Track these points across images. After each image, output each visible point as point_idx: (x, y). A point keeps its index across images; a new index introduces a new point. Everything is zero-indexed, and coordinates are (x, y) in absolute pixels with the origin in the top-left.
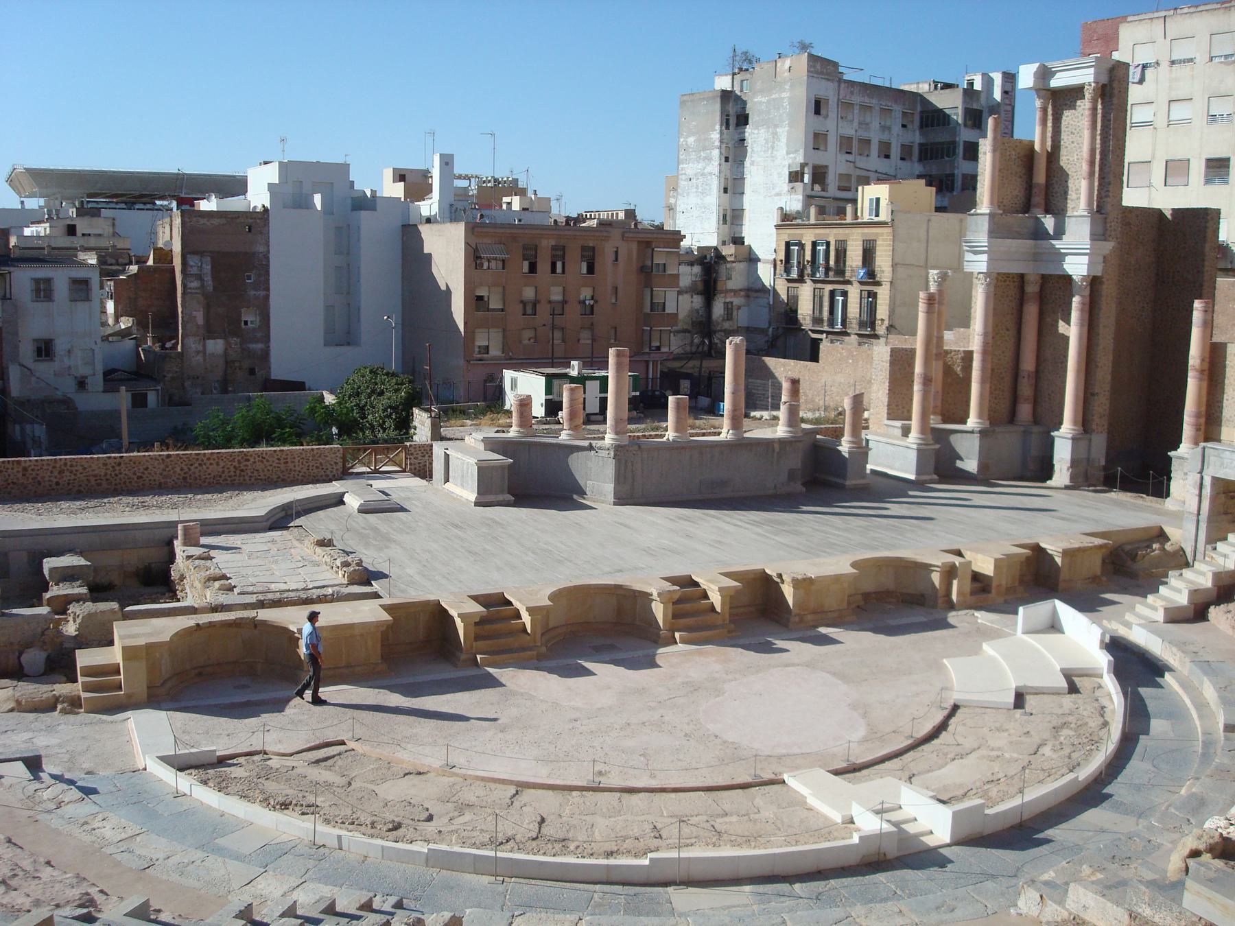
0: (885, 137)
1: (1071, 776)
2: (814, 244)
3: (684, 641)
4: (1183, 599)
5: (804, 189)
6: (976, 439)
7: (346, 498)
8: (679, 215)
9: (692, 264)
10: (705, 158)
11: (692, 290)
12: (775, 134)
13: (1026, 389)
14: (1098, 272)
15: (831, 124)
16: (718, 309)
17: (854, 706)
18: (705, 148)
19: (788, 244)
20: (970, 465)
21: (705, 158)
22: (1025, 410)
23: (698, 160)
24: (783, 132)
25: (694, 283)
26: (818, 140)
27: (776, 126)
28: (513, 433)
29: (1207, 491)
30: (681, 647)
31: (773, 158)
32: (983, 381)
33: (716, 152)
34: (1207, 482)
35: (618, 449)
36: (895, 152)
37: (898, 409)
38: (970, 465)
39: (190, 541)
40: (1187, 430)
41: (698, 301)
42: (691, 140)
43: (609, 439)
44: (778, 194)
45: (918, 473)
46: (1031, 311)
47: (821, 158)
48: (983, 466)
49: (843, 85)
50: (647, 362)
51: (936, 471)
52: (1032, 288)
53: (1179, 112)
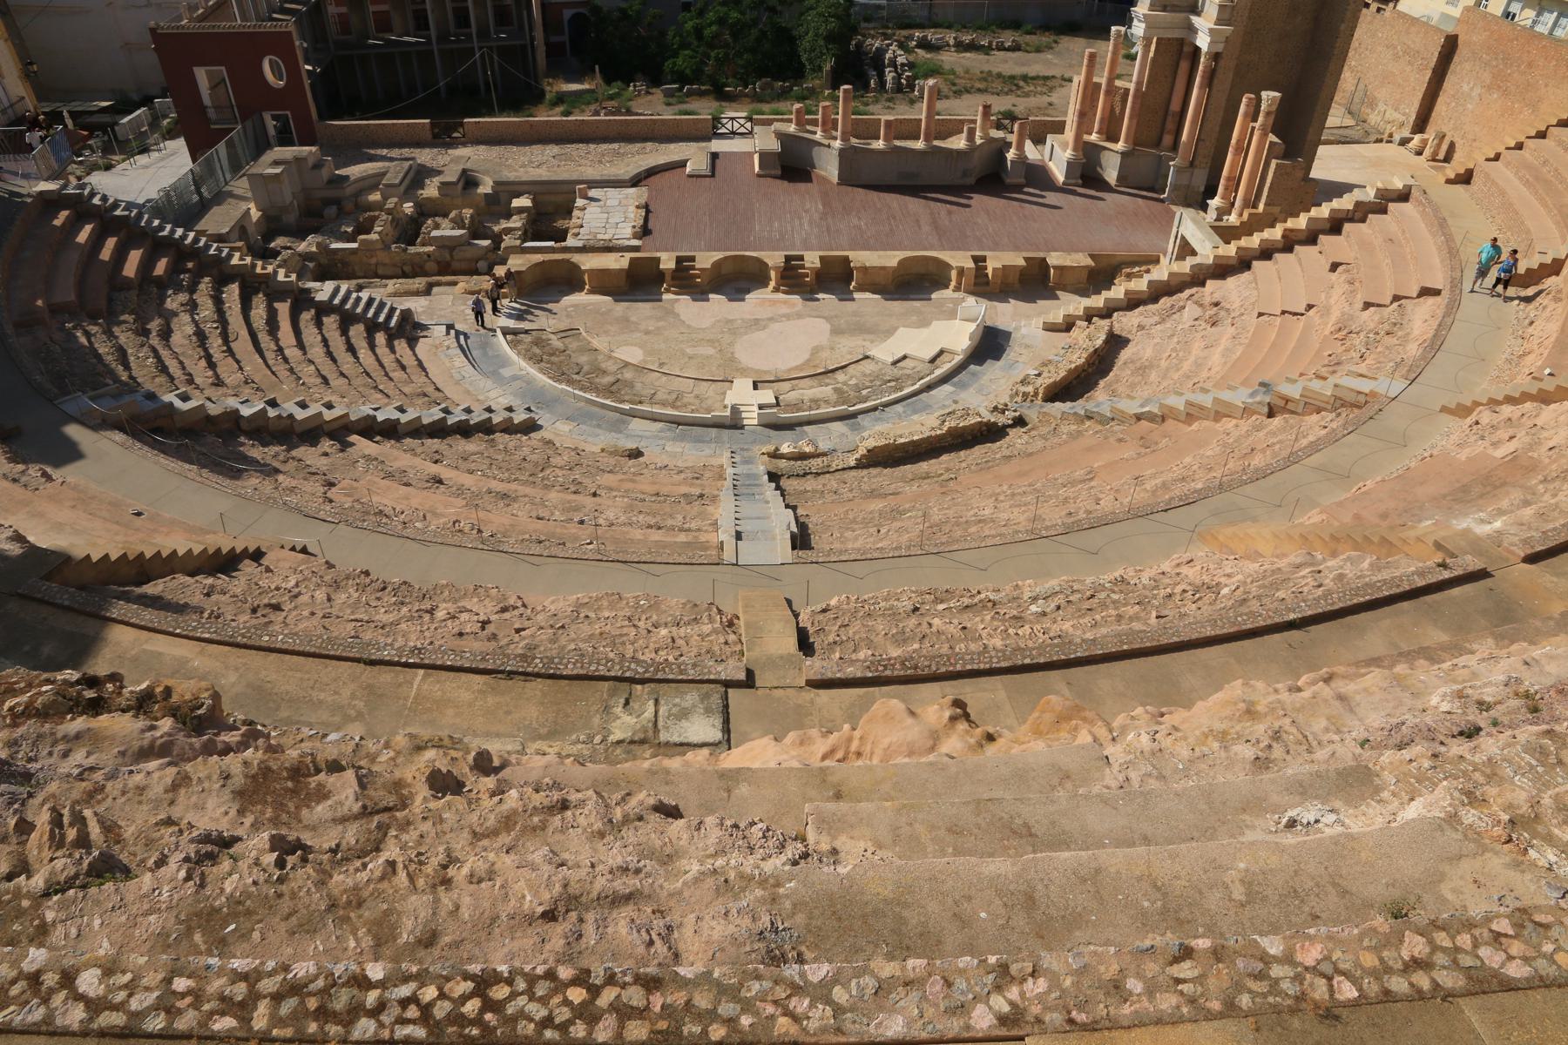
3: (785, 292)
6: (1117, 160)
13: (1170, 125)
14: (1220, 48)
20: (1111, 176)
22: (1168, 140)
28: (792, 128)
30: (781, 296)
32: (1131, 118)
35: (842, 152)
38: (1111, 176)
43: (837, 144)
45: (1067, 177)
46: (1184, 65)
48: (1119, 179)
51: (1082, 177)
52: (1186, 49)
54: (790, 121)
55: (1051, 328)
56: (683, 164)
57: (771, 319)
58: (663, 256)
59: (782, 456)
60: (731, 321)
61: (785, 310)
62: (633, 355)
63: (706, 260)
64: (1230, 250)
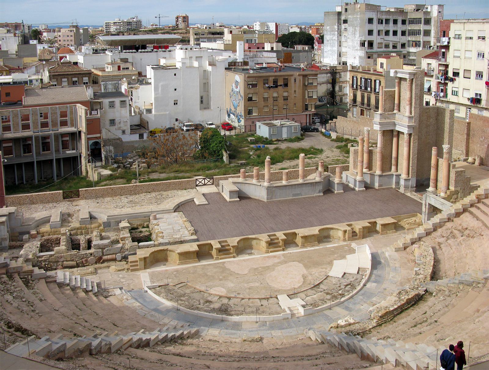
0: (395, 29)
1: (339, 300)
2: (361, 78)
4: (401, 245)
5: (365, 49)
7: (195, 200)
8: (325, 53)
9: (327, 73)
10: (333, 34)
11: (327, 82)
12: (355, 29)
15: (375, 27)
16: (337, 88)
17: (303, 276)
18: (333, 31)
19: (353, 77)
21: (333, 34)
23: (330, 34)
24: (358, 29)
25: (328, 80)
26: (370, 32)
27: (355, 27)
29: (427, 206)
31: (355, 37)
33: (336, 33)
34: (427, 204)
36: (399, 33)
37: (355, 167)
39: (155, 218)
40: (432, 184)
41: (330, 86)
42: (328, 27)
44: (357, 50)
47: (370, 38)
49: (379, 13)
50: (307, 115)
53: (468, 54)
54: (239, 177)
55: (397, 250)
56: (192, 201)
57: (273, 265)
58: (212, 242)
59: (342, 327)
60: (256, 269)
61: (276, 260)
62: (222, 291)
63: (233, 241)
64: (459, 206)
